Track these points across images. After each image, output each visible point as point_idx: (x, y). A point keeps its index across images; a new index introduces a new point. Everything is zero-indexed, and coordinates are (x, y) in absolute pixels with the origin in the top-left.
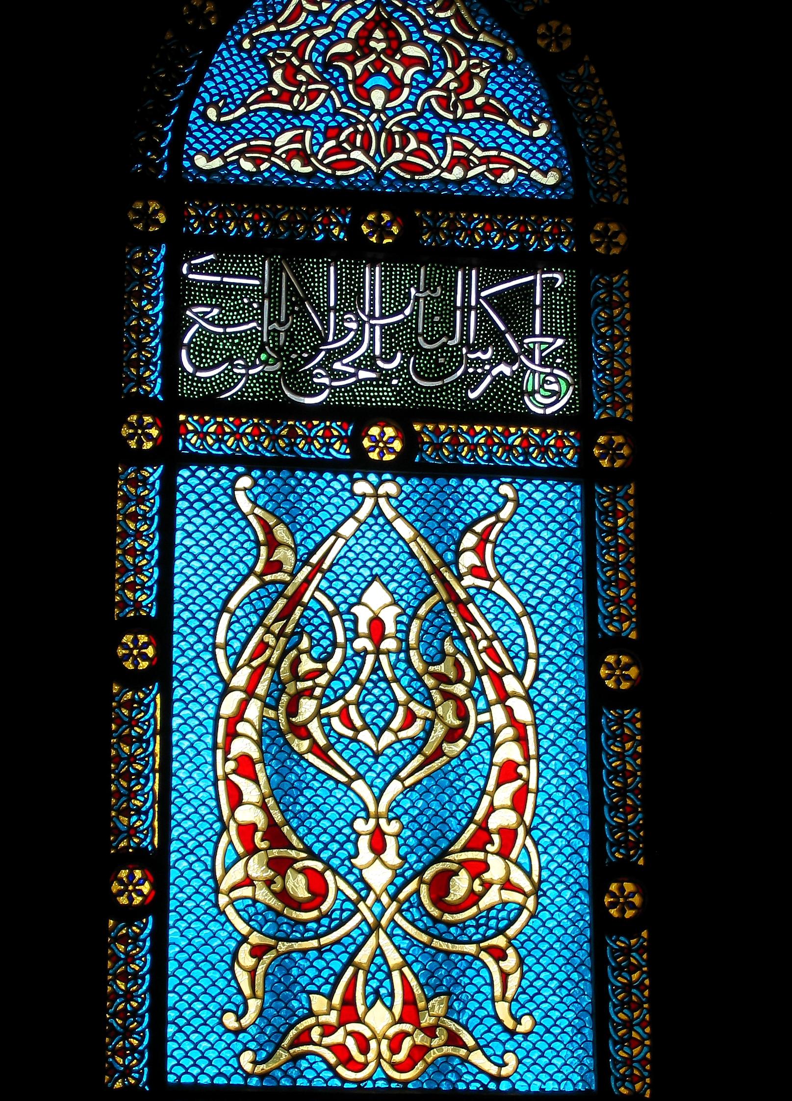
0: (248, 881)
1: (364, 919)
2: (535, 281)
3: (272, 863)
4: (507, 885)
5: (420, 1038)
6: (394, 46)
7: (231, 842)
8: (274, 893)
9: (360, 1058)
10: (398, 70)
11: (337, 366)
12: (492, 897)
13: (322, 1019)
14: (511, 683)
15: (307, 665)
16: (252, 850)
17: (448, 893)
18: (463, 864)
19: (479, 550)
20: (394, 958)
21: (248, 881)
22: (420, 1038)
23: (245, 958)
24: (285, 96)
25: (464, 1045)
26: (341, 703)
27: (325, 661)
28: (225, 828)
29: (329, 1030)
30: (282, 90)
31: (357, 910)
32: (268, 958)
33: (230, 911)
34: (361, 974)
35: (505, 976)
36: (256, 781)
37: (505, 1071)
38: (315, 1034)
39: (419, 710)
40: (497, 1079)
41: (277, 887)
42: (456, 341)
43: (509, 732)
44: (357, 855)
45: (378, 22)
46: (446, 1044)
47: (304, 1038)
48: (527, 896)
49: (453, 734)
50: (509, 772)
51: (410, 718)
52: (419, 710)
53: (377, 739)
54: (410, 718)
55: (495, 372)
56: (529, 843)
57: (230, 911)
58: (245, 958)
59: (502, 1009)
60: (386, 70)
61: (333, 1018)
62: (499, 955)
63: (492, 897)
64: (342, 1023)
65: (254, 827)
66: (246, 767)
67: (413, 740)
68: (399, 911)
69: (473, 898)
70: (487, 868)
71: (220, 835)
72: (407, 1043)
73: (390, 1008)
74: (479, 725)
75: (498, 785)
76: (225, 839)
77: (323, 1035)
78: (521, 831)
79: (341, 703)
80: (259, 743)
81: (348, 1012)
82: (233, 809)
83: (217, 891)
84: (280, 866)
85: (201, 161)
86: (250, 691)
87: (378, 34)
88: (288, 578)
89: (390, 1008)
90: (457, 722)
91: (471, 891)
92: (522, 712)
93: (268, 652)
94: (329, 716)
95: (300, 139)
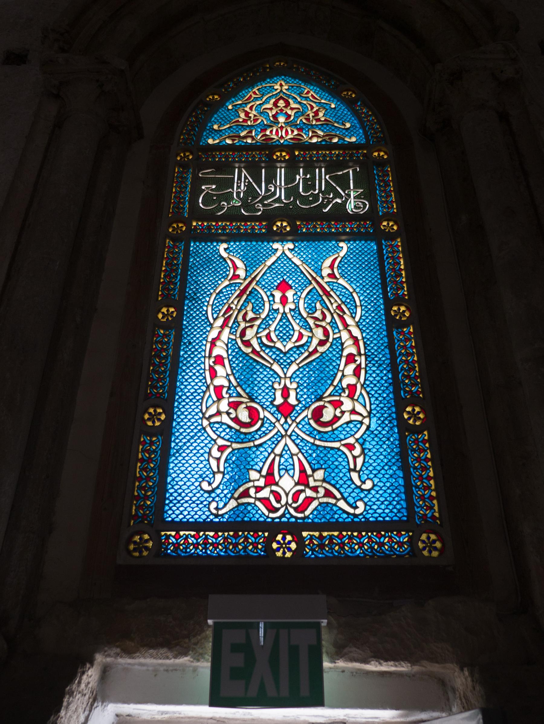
0: (219, 413)
1: (279, 431)
2: (349, 171)
3: (231, 405)
4: (353, 412)
5: (309, 493)
7: (210, 396)
8: (232, 419)
10: (289, 112)
12: (346, 417)
13: (257, 484)
14: (349, 321)
15: (250, 315)
16: (220, 397)
17: (322, 416)
18: (330, 402)
19: (332, 267)
20: (294, 449)
21: (219, 413)
22: (309, 493)
23: (215, 453)
25: (334, 497)
26: (267, 331)
28: (208, 387)
29: (259, 489)
30: (244, 119)
31: (275, 427)
33: (208, 429)
34: (277, 458)
35: (355, 458)
36: (224, 365)
37: (358, 512)
38: (252, 492)
39: (305, 333)
40: (356, 516)
41: (233, 416)
42: (317, 192)
43: (351, 342)
44: (275, 399)
46: (324, 496)
47: (246, 494)
48: (364, 417)
50: (351, 358)
51: (301, 336)
52: (305, 333)
53: (285, 346)
54: (301, 336)
55: (334, 202)
56: (364, 392)
57: (208, 429)
59: (354, 476)
60: (284, 112)
61: (262, 482)
62: (351, 447)
63: (346, 417)
64: (266, 485)
65: (222, 387)
66: (219, 360)
67: (302, 346)
68: (297, 426)
69: (336, 419)
70: (341, 403)
71: (204, 392)
73: (293, 477)
74: (334, 339)
75: (347, 364)
76: (207, 394)
77: (257, 492)
78: (359, 386)
79: (267, 331)
80: (227, 351)
81: (270, 479)
82: (212, 379)
84: (234, 405)
85: (210, 141)
86: (222, 327)
87: (281, 103)
88: (242, 281)
89: (293, 477)
90: (324, 338)
91: (335, 416)
92: (356, 332)
93: (232, 312)
94: (260, 338)
95: (251, 132)
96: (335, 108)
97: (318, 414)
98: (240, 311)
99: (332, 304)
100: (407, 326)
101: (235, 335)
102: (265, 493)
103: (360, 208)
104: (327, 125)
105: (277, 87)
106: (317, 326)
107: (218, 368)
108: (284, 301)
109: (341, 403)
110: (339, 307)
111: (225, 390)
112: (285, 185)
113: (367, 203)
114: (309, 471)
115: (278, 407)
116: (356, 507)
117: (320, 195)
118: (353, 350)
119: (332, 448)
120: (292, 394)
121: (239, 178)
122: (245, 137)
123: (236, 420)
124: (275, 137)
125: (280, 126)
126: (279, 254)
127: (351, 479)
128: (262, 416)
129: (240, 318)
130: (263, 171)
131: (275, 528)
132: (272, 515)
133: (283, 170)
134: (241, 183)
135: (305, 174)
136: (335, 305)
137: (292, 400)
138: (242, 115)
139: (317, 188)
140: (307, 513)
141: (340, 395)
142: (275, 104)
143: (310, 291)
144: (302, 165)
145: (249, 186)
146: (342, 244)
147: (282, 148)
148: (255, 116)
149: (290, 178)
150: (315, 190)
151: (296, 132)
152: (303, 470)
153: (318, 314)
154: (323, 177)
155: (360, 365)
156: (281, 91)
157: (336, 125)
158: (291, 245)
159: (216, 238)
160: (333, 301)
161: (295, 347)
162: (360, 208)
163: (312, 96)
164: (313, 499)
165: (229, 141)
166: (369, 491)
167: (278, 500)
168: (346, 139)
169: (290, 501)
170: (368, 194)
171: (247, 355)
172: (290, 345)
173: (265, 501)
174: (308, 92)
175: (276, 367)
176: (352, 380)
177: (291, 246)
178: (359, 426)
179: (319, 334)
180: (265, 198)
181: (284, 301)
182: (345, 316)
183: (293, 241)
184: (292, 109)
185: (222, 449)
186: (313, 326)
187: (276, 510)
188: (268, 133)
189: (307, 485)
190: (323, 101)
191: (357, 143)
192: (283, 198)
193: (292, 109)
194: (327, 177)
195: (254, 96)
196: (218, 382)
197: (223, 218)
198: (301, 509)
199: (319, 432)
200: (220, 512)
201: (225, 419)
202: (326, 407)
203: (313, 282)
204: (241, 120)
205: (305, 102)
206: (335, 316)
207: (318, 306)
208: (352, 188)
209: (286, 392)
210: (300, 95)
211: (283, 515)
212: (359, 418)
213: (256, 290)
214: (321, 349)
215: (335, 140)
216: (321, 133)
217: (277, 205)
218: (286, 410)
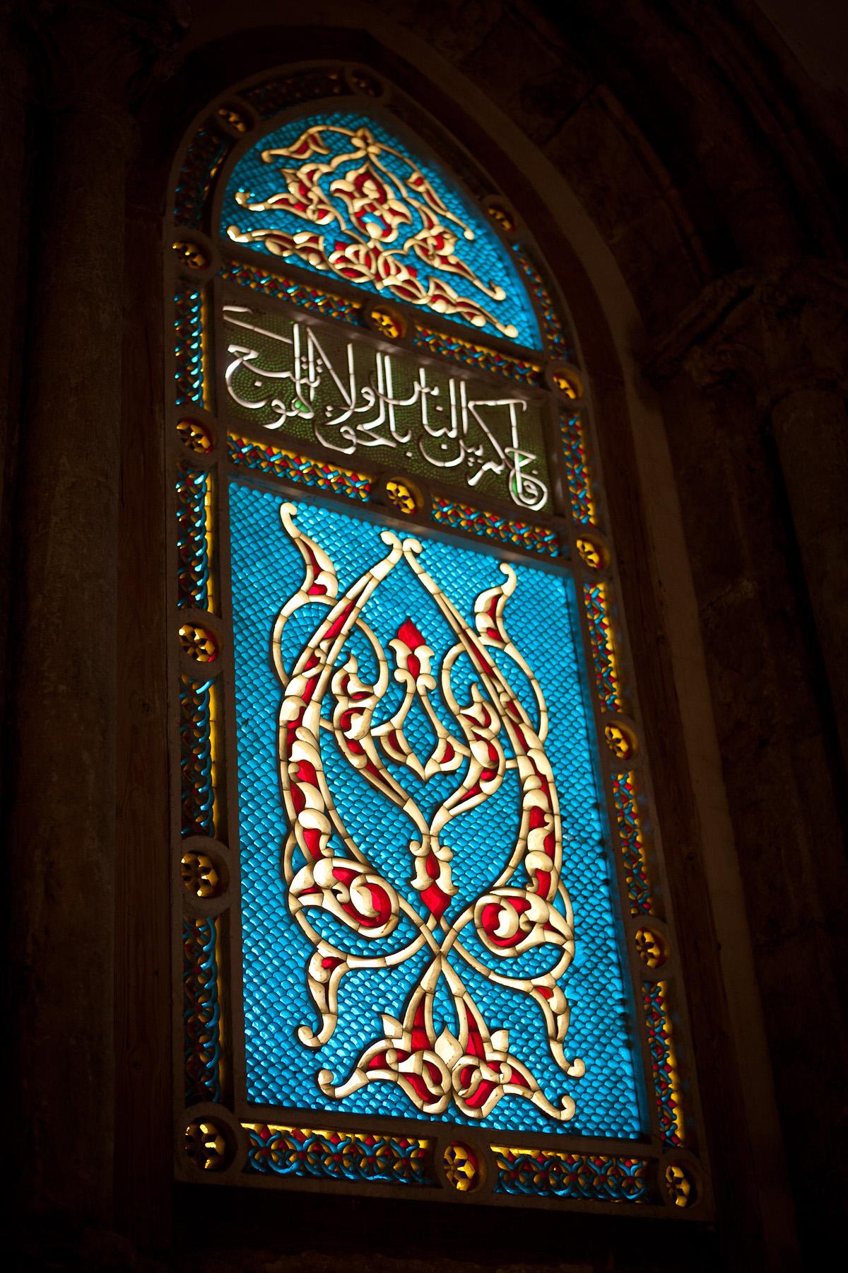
0: (316, 889)
1: (426, 943)
4: (547, 926)
6: (383, 199)
9: (433, 1091)
10: (388, 218)
11: (359, 428)
12: (535, 936)
15: (353, 687)
16: (317, 856)
17: (497, 926)
19: (491, 612)
22: (487, 1074)
23: (316, 971)
27: (372, 684)
29: (403, 1056)
31: (419, 933)
32: (338, 970)
33: (299, 917)
35: (555, 1015)
36: (316, 785)
37: (566, 1115)
38: (390, 1058)
39: (458, 748)
40: (560, 1123)
44: (414, 876)
45: (367, 176)
49: (488, 774)
50: (537, 818)
51: (449, 754)
52: (458, 748)
54: (449, 754)
55: (486, 467)
58: (316, 971)
59: (556, 1049)
60: (377, 213)
61: (404, 1044)
63: (535, 936)
64: (414, 1051)
66: (307, 772)
69: (521, 935)
70: (527, 906)
72: (475, 1078)
75: (530, 829)
76: (289, 843)
83: (286, 893)
85: (231, 233)
86: (307, 698)
87: (369, 186)
94: (376, 740)
95: (314, 240)
96: (473, 242)
97: (490, 917)
98: (334, 671)
99: (498, 695)
100: (624, 772)
101: (331, 720)
102: (410, 1065)
103: (532, 496)
104: (462, 277)
105: (357, 142)
106: (478, 738)
107: (305, 787)
109: (527, 906)
110: (510, 705)
111: (323, 841)
112: (395, 398)
113: (545, 489)
114: (483, 1032)
115: (419, 893)
116: (561, 1108)
117: (461, 443)
119: (515, 991)
120: (445, 871)
121: (304, 352)
122: (306, 250)
124: (363, 269)
125: (371, 245)
126: (394, 557)
127: (550, 1054)
128: (394, 908)
129: (336, 689)
130: (350, 348)
132: (430, 1109)
133: (387, 359)
134: (307, 363)
135: (430, 385)
136: (504, 699)
137: (444, 883)
138: (293, 188)
139: (454, 424)
140: (485, 1109)
141: (523, 888)
142: (359, 183)
143: (456, 659)
144: (427, 362)
145: (324, 376)
146: (505, 568)
148: (321, 202)
149: (403, 390)
150: (450, 429)
151: (404, 275)
153: (474, 711)
154: (464, 404)
155: (552, 834)
156: (366, 158)
157: (477, 283)
158: (412, 544)
159: (283, 486)
160: (499, 690)
161: (440, 773)
162: (532, 496)
163: (428, 192)
164: (493, 1085)
165: (273, 248)
166: (577, 1079)
167: (437, 1080)
168: (499, 327)
169: (456, 1086)
170: (548, 470)
171: (356, 771)
172: (431, 768)
174: (419, 182)
175: (410, 808)
177: (417, 549)
178: (555, 953)
179: (480, 752)
180: (356, 419)
181: (414, 666)
182: (521, 726)
183: (421, 537)
184: (394, 212)
185: (330, 964)
186: (470, 736)
187: (433, 1099)
188: (349, 252)
189: (481, 1056)
190: (449, 215)
191: (517, 342)
192: (393, 427)
193: (394, 212)
194: (471, 405)
195: (313, 147)
196: (309, 820)
197: (276, 438)
198: (477, 1101)
199: (495, 956)
200: (340, 1092)
201: (329, 903)
202: (503, 909)
203: (461, 637)
204: (292, 201)
205: (415, 204)
206: (505, 720)
207: (476, 696)
208: (516, 444)
209: (433, 868)
210: (404, 179)
211: (445, 1112)
212: (552, 938)
213: (360, 629)
214: (488, 787)
215: (478, 322)
216: (451, 294)
217: (380, 441)
218: (434, 902)
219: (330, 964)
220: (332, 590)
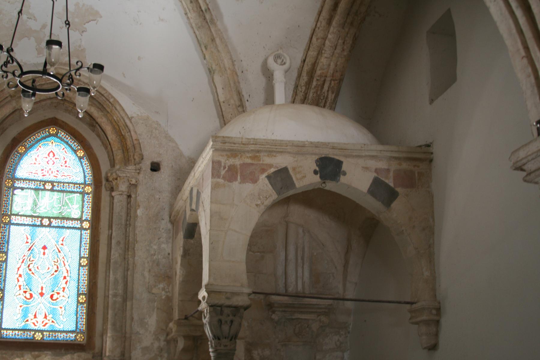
6: (54, 155)
10: (55, 161)
15: (32, 259)
22: (46, 321)
24: (35, 164)
38: (29, 320)
49: (56, 271)
52: (50, 267)
69: (57, 298)
97: (52, 296)
107: (20, 278)
108: (44, 254)
118: (66, 275)
120: (44, 289)
123: (25, 297)
131: (36, 331)
147: (49, 182)
152: (46, 315)
173: (34, 323)
176: (64, 285)
196: (20, 283)
214: (55, 273)
219: (21, 306)
220: (30, 242)
